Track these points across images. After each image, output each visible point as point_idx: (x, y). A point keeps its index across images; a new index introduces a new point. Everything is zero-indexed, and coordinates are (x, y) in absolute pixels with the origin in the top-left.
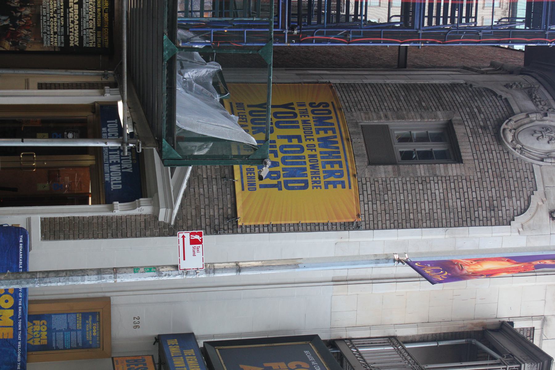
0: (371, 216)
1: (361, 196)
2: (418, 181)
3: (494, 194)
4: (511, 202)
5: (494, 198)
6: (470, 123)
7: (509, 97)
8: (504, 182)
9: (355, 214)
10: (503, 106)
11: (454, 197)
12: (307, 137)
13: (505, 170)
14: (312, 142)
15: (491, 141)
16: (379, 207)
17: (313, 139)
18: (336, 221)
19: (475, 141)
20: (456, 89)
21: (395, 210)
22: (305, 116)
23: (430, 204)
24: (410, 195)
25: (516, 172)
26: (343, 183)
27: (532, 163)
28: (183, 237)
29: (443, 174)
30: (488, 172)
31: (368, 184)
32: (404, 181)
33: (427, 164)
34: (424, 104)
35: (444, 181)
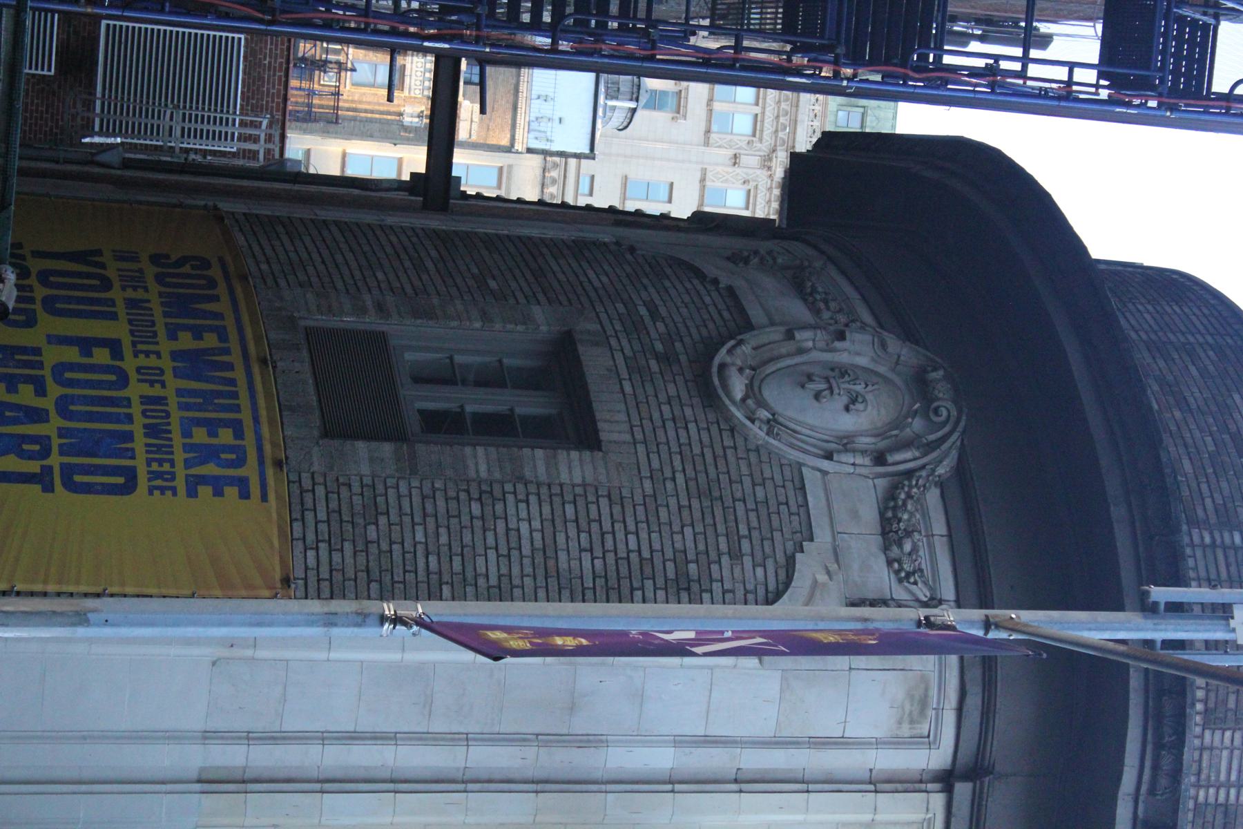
2: (468, 491)
3: (690, 544)
4: (737, 571)
5: (691, 556)
6: (625, 342)
7: (739, 283)
8: (718, 512)
9: (278, 576)
10: (721, 306)
11: (573, 545)
12: (140, 347)
14: (153, 361)
15: (684, 394)
16: (349, 560)
17: (158, 355)
19: (640, 391)
20: (587, 254)
21: (398, 571)
22: (135, 288)
23: (503, 561)
24: (442, 531)
25: (754, 485)
27: (800, 465)
29: (543, 476)
30: (674, 479)
31: (320, 491)
32: (427, 490)
33: (498, 446)
34: (493, 284)
35: (544, 497)
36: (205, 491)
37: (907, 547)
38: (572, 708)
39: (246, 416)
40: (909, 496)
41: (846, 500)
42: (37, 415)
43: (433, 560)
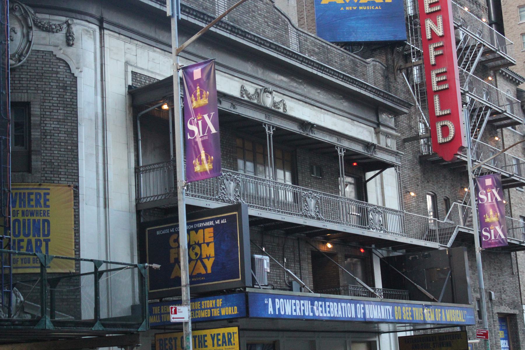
0: (69, 177)
1: (55, 182)
3: (55, 84)
8: (46, 75)
11: (56, 114)
13: (37, 71)
18: (73, 202)
26: (45, 194)
28: (173, 318)
29: (39, 118)
30: (38, 85)
31: (46, 175)
32: (44, 149)
35: (44, 119)
36: (48, 203)
37: (54, 27)
38: (91, 120)
39: (27, 191)
40: (40, 22)
41: (41, 40)
42: (29, 242)
43: (62, 150)
